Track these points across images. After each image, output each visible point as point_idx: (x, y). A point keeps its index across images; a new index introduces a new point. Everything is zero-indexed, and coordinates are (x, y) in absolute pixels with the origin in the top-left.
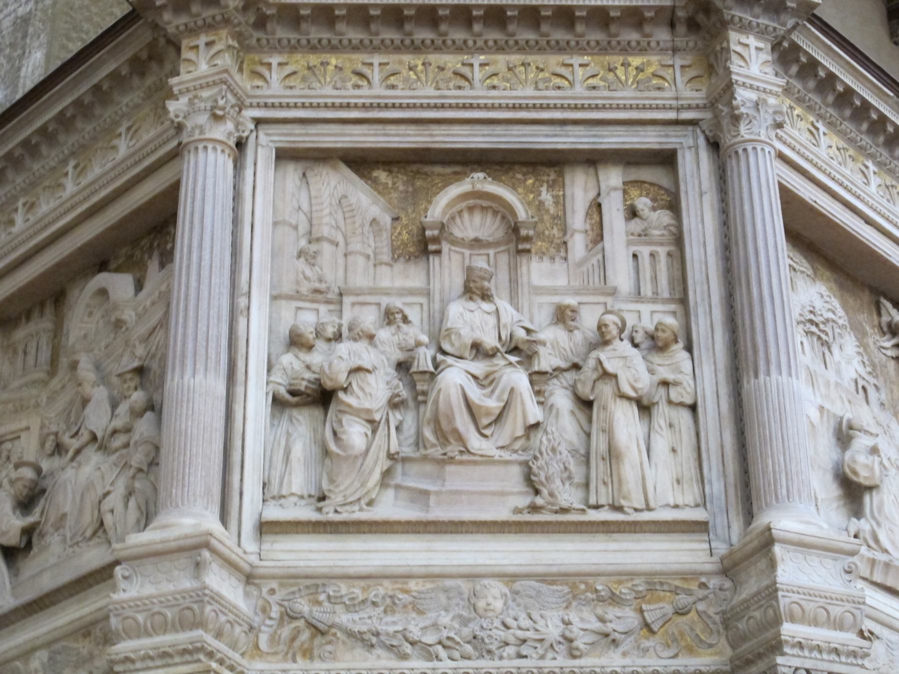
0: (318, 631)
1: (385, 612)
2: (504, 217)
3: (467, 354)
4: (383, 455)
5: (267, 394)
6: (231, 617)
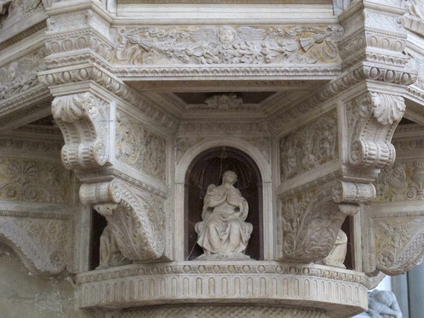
0: (145, 50)
1: (177, 41)
6: (103, 43)
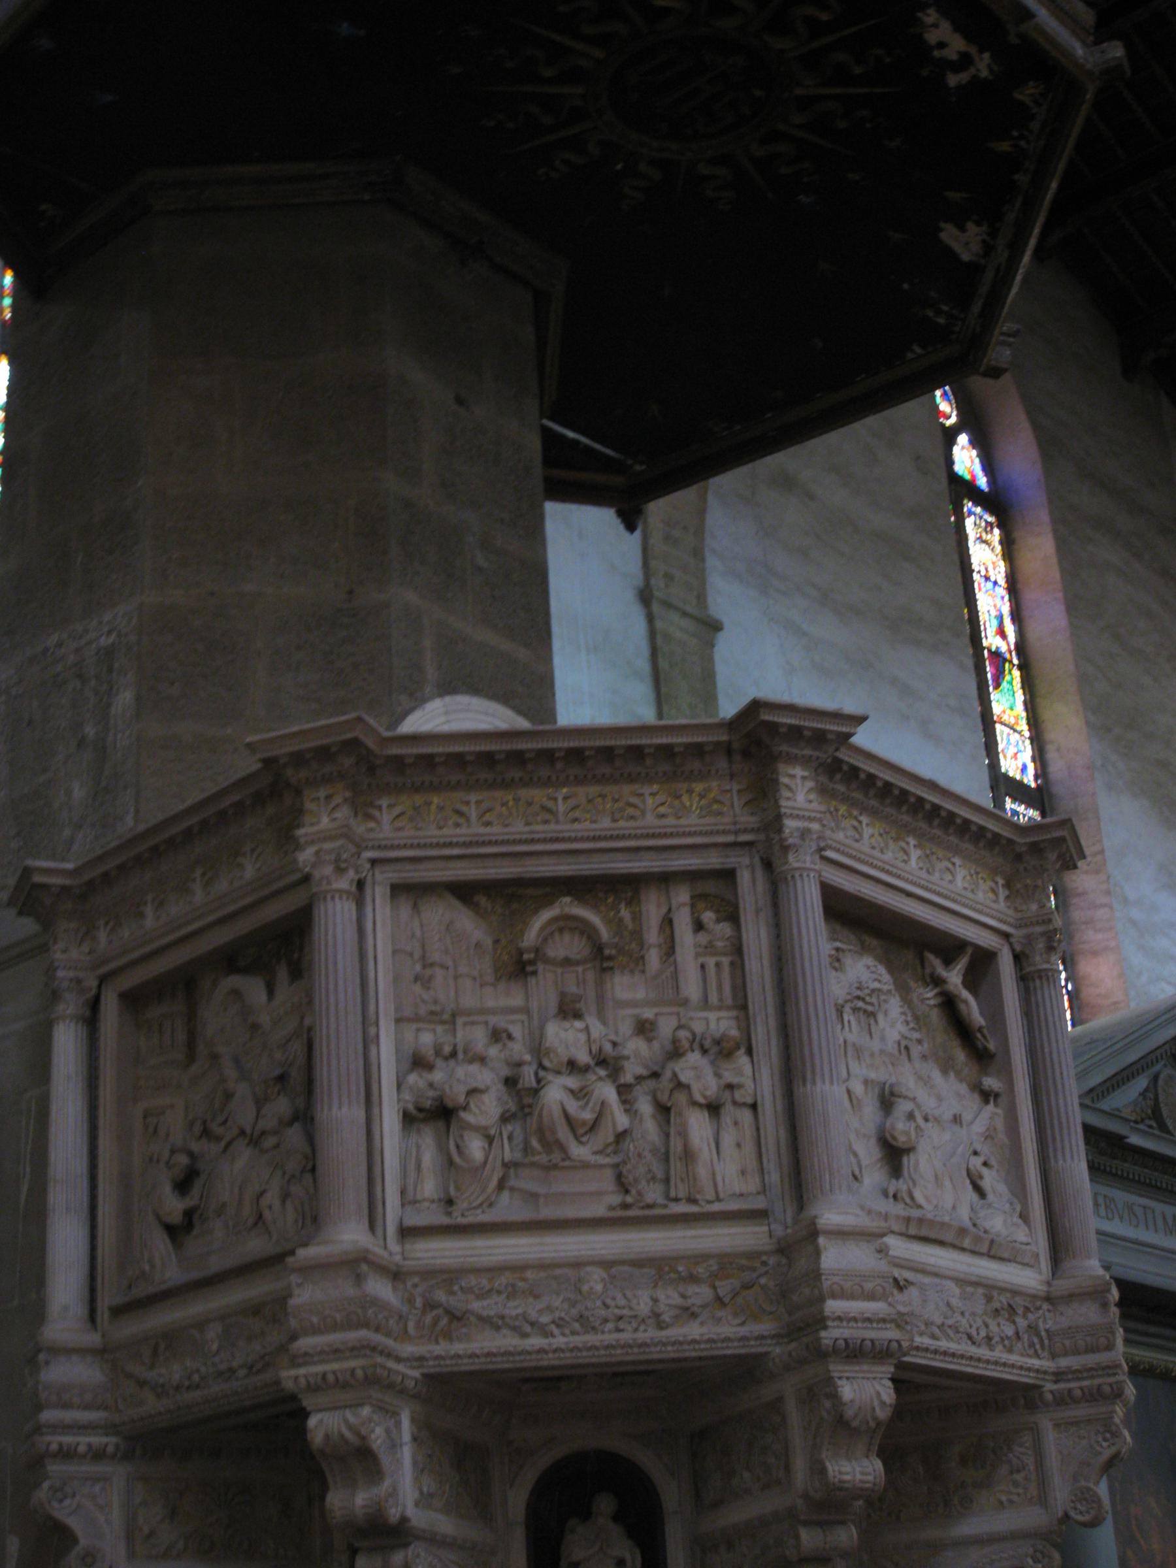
0: (456, 1317)
1: (508, 1298)
2: (589, 937)
3: (564, 1070)
4: (499, 1163)
5: (399, 1110)
